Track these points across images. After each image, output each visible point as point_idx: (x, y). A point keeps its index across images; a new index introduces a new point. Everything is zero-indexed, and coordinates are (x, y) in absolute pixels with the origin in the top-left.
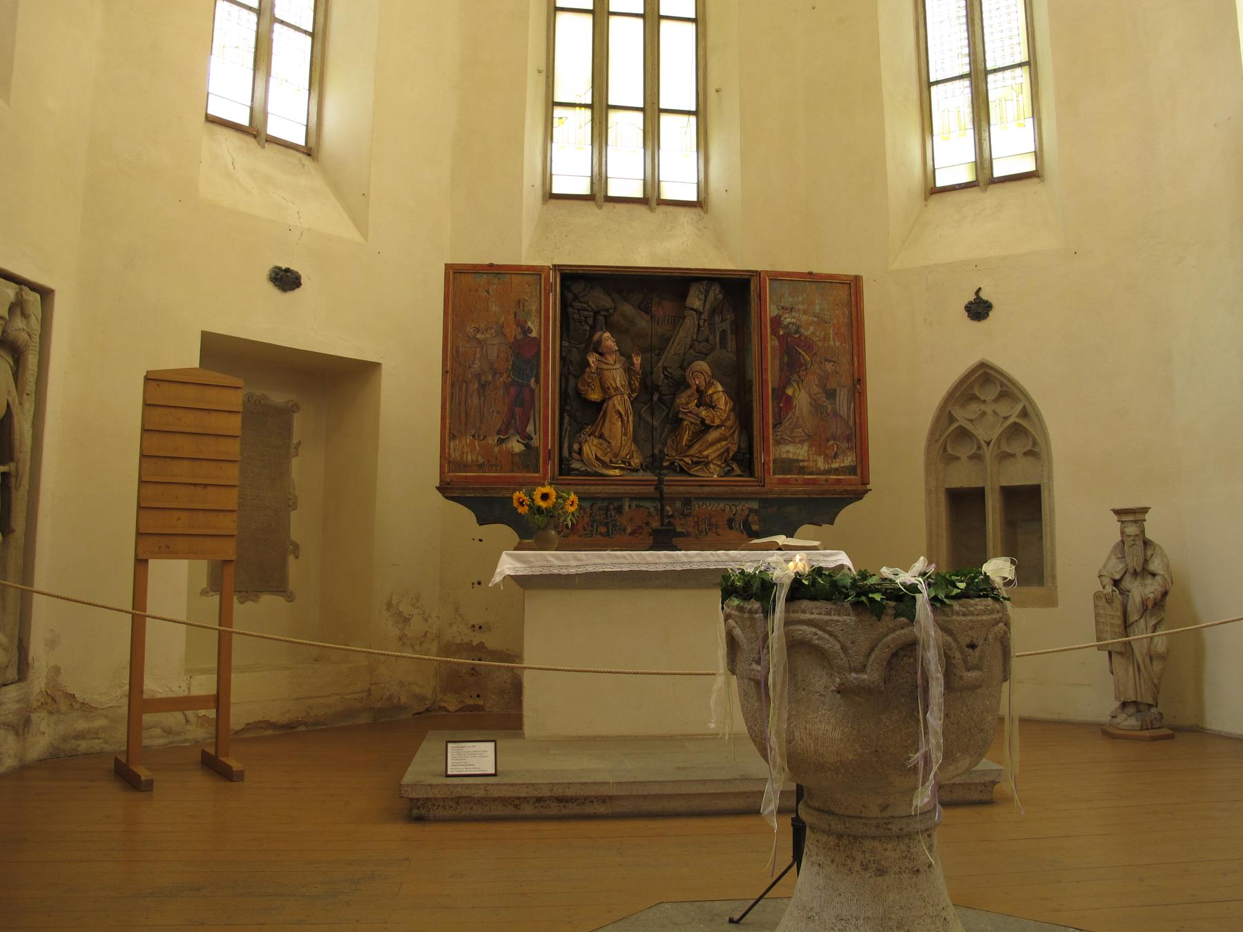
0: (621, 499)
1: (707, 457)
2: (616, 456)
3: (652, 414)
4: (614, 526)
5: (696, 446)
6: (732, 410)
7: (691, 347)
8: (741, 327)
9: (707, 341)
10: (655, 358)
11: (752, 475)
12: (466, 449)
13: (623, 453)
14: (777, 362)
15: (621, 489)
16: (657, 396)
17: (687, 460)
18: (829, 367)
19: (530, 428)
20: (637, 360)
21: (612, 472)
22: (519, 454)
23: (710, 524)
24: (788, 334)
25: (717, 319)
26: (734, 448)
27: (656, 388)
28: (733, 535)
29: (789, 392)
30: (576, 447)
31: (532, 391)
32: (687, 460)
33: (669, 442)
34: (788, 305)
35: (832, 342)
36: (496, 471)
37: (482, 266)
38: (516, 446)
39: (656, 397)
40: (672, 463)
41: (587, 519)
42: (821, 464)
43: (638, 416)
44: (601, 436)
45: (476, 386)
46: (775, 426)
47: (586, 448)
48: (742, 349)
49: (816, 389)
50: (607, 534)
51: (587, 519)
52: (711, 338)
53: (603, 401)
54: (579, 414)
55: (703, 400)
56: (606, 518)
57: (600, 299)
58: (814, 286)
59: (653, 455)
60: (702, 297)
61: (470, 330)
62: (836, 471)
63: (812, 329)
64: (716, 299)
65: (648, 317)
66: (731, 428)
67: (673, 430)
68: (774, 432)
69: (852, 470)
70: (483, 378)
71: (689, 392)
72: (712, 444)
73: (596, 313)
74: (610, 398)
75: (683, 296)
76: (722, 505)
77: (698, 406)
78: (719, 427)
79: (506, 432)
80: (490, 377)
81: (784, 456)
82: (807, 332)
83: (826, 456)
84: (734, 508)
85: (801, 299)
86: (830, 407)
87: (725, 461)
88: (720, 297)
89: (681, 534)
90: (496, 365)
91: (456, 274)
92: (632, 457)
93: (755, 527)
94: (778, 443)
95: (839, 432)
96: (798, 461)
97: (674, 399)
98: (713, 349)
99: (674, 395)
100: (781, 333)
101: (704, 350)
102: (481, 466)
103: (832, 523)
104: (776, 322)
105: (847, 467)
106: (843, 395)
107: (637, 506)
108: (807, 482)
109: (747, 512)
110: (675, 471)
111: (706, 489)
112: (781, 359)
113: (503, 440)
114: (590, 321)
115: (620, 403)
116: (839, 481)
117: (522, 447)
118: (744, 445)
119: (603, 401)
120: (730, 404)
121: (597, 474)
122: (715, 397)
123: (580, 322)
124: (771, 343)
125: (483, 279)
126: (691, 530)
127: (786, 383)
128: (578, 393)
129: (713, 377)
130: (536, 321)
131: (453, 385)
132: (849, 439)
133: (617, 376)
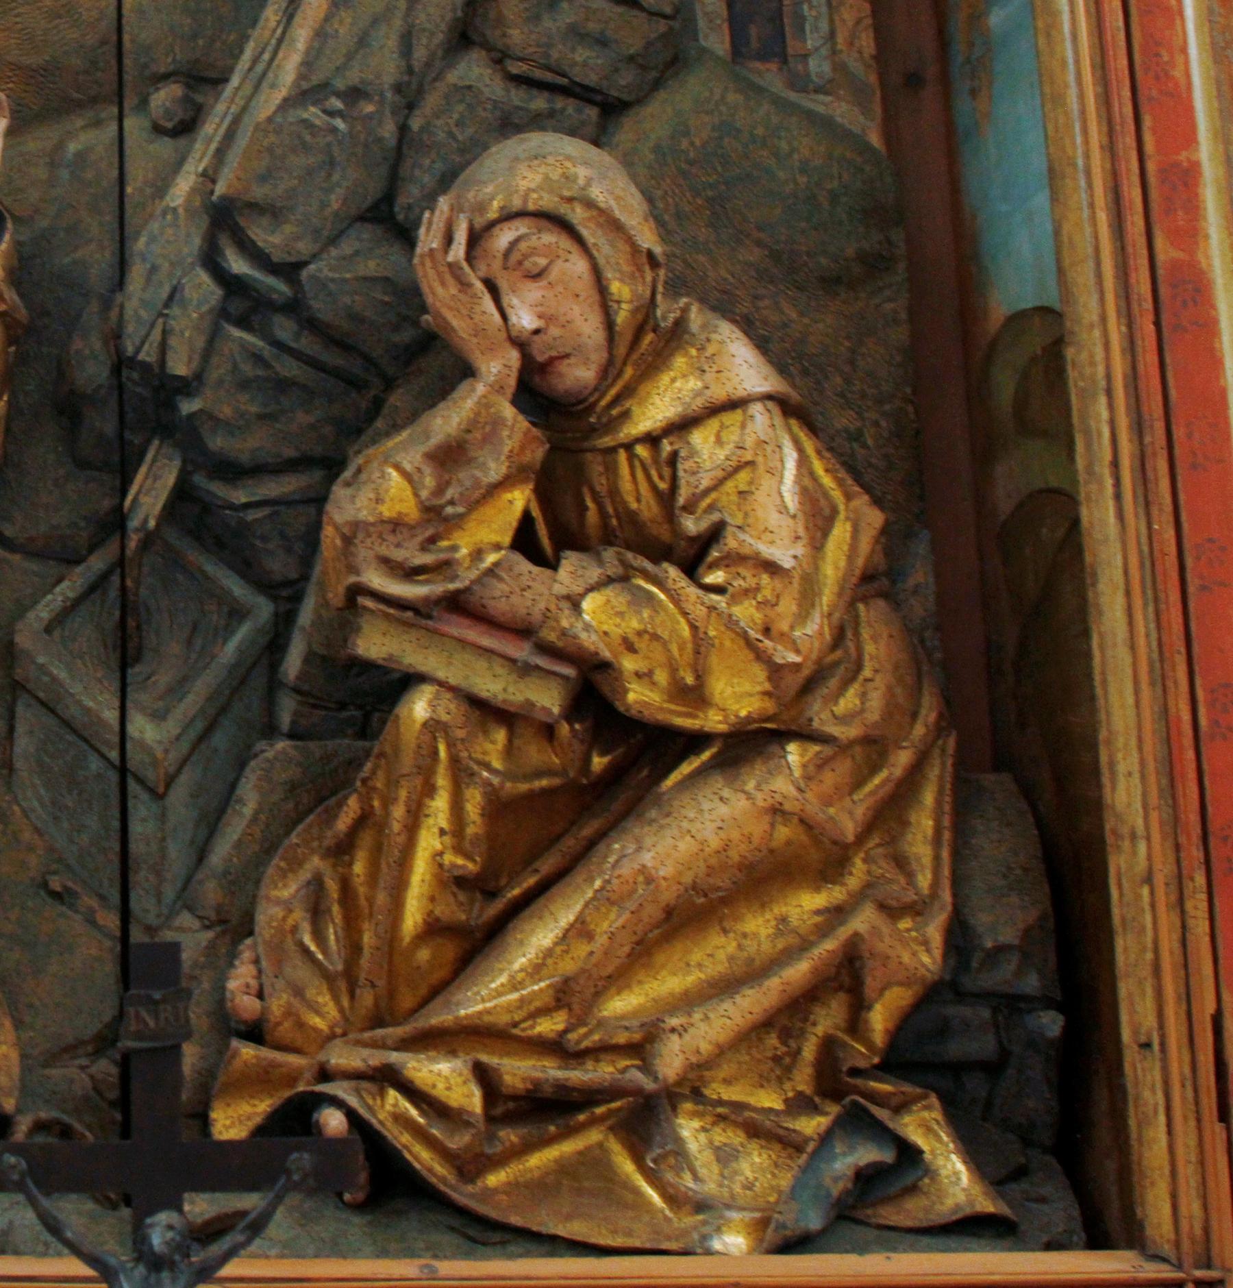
1: (641, 1049)
3: (126, 653)
5: (539, 937)
17: (442, 1074)
27: (151, 403)
32: (442, 1074)
39: (151, 490)
40: (295, 1118)
55: (583, 481)
66: (874, 747)
71: (447, 421)
72: (690, 913)
78: (747, 745)
87: (832, 1081)
99: (332, 466)
110: (326, 1183)
122: (707, 449)
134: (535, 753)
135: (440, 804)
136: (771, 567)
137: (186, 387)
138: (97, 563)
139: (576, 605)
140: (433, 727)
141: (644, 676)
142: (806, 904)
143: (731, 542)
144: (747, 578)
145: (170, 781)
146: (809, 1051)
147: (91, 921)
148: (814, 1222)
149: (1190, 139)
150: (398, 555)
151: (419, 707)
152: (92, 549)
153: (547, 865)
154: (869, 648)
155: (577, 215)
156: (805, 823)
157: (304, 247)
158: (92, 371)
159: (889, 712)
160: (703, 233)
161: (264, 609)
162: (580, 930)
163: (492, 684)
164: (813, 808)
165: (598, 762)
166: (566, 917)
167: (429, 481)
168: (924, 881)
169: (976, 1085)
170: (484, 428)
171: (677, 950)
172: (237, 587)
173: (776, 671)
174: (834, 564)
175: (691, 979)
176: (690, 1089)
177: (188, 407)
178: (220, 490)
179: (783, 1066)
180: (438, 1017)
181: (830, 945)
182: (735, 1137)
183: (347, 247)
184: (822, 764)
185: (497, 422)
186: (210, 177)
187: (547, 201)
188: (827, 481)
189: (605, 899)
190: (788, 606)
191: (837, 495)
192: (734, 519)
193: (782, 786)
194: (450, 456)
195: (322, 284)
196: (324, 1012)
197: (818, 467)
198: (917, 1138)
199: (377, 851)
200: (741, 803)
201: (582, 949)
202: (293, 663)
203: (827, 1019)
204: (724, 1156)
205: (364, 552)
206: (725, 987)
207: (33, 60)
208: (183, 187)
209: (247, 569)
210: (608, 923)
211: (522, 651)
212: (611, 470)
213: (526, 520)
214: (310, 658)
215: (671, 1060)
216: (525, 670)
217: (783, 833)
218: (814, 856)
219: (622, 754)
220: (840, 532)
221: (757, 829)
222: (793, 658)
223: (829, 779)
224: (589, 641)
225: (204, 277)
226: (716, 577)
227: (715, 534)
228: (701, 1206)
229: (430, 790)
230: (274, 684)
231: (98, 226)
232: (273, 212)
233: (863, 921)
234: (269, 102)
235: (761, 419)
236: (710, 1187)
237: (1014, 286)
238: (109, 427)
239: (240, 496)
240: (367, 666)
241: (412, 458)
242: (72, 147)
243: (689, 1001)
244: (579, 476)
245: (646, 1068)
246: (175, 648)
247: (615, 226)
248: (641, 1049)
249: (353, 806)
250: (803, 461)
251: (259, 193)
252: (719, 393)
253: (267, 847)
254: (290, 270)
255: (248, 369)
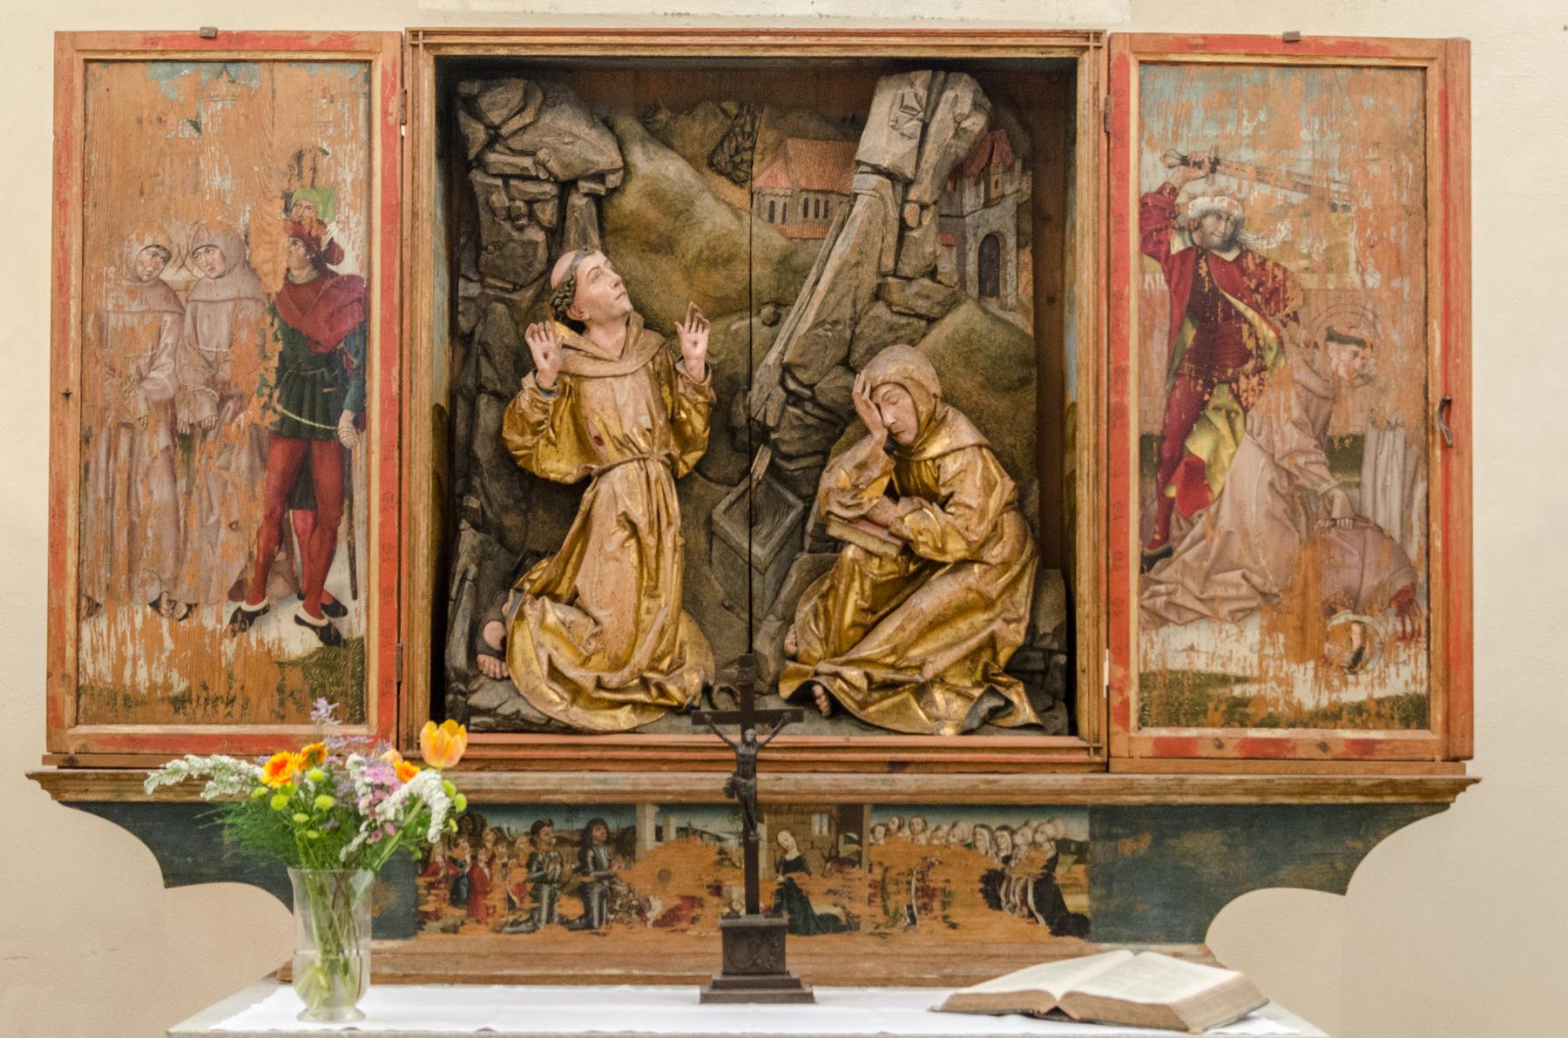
0: (625, 808)
2: (617, 664)
3: (752, 521)
4: (609, 896)
5: (888, 629)
6: (1017, 504)
7: (878, 295)
8: (1045, 223)
9: (932, 273)
10: (763, 332)
11: (1073, 730)
12: (131, 647)
13: (641, 657)
14: (1159, 347)
15: (620, 781)
16: (756, 459)
17: (854, 674)
18: (1340, 359)
19: (337, 579)
20: (696, 343)
21: (601, 720)
22: (302, 664)
23: (926, 892)
24: (1198, 252)
25: (971, 198)
26: (1014, 635)
27: (762, 434)
28: (1003, 926)
29: (1200, 446)
30: (491, 633)
31: (344, 455)
32: (854, 674)
33: (804, 610)
34: (1202, 151)
35: (1353, 277)
36: (228, 719)
37: (175, 37)
38: (290, 633)
39: (760, 465)
41: (519, 874)
42: (1307, 692)
43: (699, 523)
44: (573, 600)
45: (162, 440)
46: (1148, 563)
47: (523, 642)
48: (1050, 300)
49: (1294, 438)
50: (586, 923)
51: (519, 874)
52: (947, 266)
53: (585, 481)
54: (511, 521)
55: (907, 478)
56: (582, 869)
57: (571, 139)
58: (1296, 80)
59: (750, 659)
60: (913, 126)
61: (140, 254)
62: (1359, 714)
63: (1283, 230)
64: (959, 132)
65: (738, 195)
66: (1006, 565)
67: (820, 571)
68: (1145, 584)
69: (1414, 711)
70: (184, 416)
71: (862, 451)
72: (938, 623)
73: (566, 187)
74: (602, 473)
75: (854, 124)
76: (965, 827)
77: (891, 493)
78: (961, 565)
79: (261, 591)
80: (206, 413)
81: (1178, 663)
82: (1261, 243)
83: (1325, 661)
84: (1005, 839)
85: (1247, 128)
86: (1339, 496)
88: (976, 123)
89: (829, 925)
90: (225, 373)
91: (87, 62)
92: (678, 664)
93: (1076, 902)
94: (1156, 619)
95: (1370, 581)
96: (1224, 680)
97: (822, 467)
98: (950, 304)
99: (823, 456)
100: (1177, 245)
101: (922, 306)
102: (179, 703)
103: (1339, 885)
104: (1160, 211)
105: (1395, 701)
106: (1386, 463)
107: (683, 832)
108: (1255, 753)
109: (1049, 851)
111: (906, 782)
112: (1175, 332)
113: (250, 618)
114: (547, 213)
115: (626, 491)
116: (1365, 749)
117: (313, 642)
118: (1047, 625)
119: (585, 481)
120: (1005, 488)
121: (549, 726)
122: (951, 466)
123: (511, 217)
124: (1146, 281)
125: (173, 84)
126: (859, 909)
127: (1191, 415)
128: (506, 458)
129: (947, 398)
130: (356, 220)
131: (86, 439)
132: (1404, 603)
133: (622, 401)
134: (890, 567)
135: (856, 585)
136: (969, 507)
137: (773, 430)
138: (742, 487)
139: (902, 519)
140: (854, 561)
141: (925, 543)
142: (980, 617)
143: (956, 498)
144: (961, 511)
145: (766, 569)
146: (980, 667)
147: (738, 616)
148: (975, 724)
149: (1127, 357)
150: (844, 500)
151: (850, 552)
152: (740, 481)
153: (894, 603)
154: (1007, 530)
155: (908, 383)
156: (979, 593)
157: (816, 378)
158: (741, 420)
159: (1012, 552)
160: (961, 370)
161: (800, 505)
162: (902, 628)
163: (874, 546)
164: (983, 588)
165: (912, 568)
166: (898, 624)
167: (855, 476)
168: (1022, 611)
169: (1038, 679)
170: (873, 456)
171: (934, 635)
172: (791, 497)
173: (969, 543)
174: (994, 503)
175: (941, 643)
176: (939, 679)
177: (774, 436)
178: (784, 464)
179: (972, 671)
180: (854, 655)
181: (984, 634)
182: (952, 696)
183: (831, 375)
184: (985, 572)
185: (878, 456)
186: (782, 354)
187: (898, 379)
188: (994, 471)
189: (910, 619)
190: (975, 520)
191: (998, 477)
192: (957, 489)
193: (971, 580)
194: (862, 466)
195: (822, 391)
196: (818, 650)
197: (992, 467)
198: (1015, 699)
199: (836, 596)
200: (957, 586)
201: (901, 634)
202: (810, 526)
203: (986, 657)
204: (948, 702)
205: (833, 499)
206: (949, 646)
207: (718, 295)
208: (772, 357)
209: (794, 491)
210: (912, 626)
211: (883, 534)
212: (919, 468)
213: (891, 482)
214: (816, 525)
215: (929, 672)
216: (885, 542)
217: (971, 596)
218: (982, 603)
219: (919, 567)
220: (998, 489)
221: (962, 595)
222: (976, 538)
223: (989, 577)
224: (907, 532)
225: (780, 390)
226: (952, 510)
227: (951, 495)
228: (937, 719)
229: (852, 580)
230: (803, 532)
231: (743, 360)
232: (805, 367)
233: (996, 626)
234: (804, 328)
235: (970, 454)
236: (942, 713)
237: (1071, 396)
238: (746, 439)
239: (792, 467)
240: (833, 539)
241: (849, 467)
242: (734, 327)
243: (937, 651)
244: (909, 468)
245: (921, 674)
246: (768, 520)
247: (921, 386)
248: (920, 668)
249: (828, 583)
250: (986, 468)
251: (799, 361)
252: (955, 445)
253: (799, 592)
254: (811, 387)
255: (795, 422)
